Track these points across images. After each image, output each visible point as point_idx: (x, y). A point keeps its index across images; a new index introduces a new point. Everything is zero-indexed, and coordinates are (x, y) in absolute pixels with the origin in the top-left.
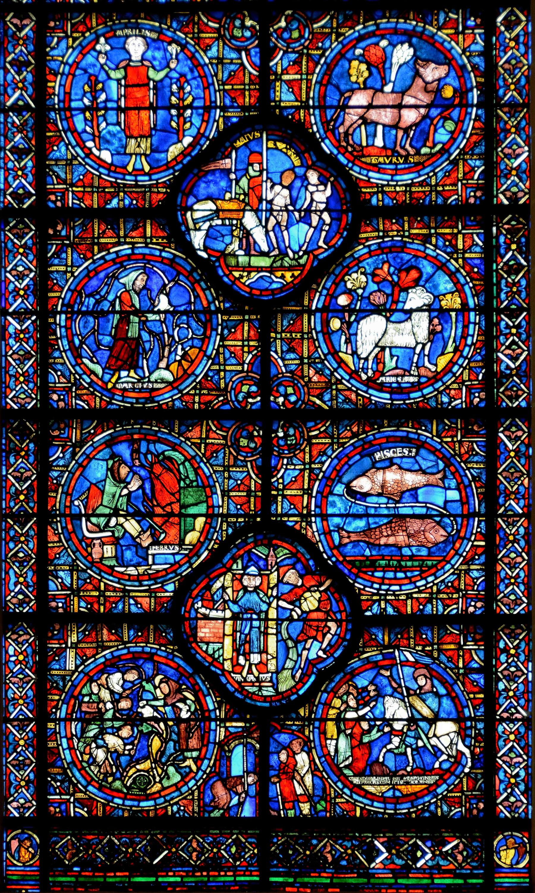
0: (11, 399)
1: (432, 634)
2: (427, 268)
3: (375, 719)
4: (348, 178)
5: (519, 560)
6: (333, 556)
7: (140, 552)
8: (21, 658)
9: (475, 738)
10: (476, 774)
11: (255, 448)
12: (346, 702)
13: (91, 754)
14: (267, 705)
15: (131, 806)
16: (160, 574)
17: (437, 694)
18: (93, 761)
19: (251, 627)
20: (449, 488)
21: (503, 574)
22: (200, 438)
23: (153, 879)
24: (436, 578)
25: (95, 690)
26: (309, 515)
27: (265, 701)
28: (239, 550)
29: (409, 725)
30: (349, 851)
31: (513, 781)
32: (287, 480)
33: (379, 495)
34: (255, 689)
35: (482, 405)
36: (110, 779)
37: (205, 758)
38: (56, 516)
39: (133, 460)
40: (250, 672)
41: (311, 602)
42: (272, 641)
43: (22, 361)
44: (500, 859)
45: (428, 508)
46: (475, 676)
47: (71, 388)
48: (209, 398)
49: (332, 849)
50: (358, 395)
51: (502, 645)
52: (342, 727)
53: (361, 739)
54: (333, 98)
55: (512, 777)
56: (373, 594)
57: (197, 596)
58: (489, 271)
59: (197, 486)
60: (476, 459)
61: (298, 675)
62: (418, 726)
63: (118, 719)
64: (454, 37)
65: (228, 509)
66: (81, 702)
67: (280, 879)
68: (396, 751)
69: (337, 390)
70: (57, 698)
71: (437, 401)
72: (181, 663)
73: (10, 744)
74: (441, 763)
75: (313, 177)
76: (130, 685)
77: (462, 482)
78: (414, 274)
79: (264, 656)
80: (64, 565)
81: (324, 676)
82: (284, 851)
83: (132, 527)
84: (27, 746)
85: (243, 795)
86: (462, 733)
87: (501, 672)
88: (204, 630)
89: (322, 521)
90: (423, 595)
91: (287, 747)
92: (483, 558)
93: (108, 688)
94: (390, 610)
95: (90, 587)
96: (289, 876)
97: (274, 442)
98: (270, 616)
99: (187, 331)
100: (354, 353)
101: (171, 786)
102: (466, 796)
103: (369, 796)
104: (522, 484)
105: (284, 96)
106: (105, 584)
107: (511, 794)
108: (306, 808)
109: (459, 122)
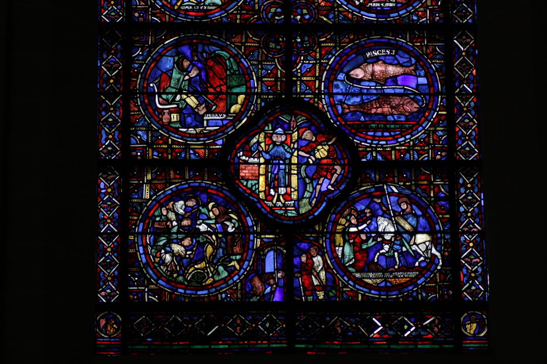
0: (104, 16)
1: (411, 174)
3: (371, 232)
5: (471, 124)
6: (338, 121)
7: (197, 118)
8: (109, 190)
9: (444, 245)
10: (446, 270)
11: (281, 49)
12: (349, 221)
13: (161, 258)
14: (292, 222)
15: (191, 294)
16: (212, 133)
18: (163, 262)
19: (279, 169)
20: (420, 76)
21: (460, 133)
22: (241, 42)
23: (207, 347)
24: (412, 136)
25: (164, 213)
26: (320, 93)
27: (289, 220)
28: (269, 117)
29: (395, 237)
30: (354, 326)
31: (473, 275)
32: (304, 71)
33: (370, 80)
34: (282, 212)
35: (441, 22)
36: (175, 275)
37: (246, 260)
38: (137, 94)
39: (192, 56)
40: (278, 200)
41: (322, 152)
42: (294, 180)
44: (466, 330)
45: (405, 89)
46: (443, 203)
47: (148, 8)
48: (247, 16)
49: (341, 324)
50: (353, 14)
51: (461, 181)
52: (347, 238)
53: (361, 246)
55: (472, 272)
56: (367, 147)
57: (239, 148)
59: (239, 74)
60: (438, 57)
61: (314, 202)
62: (402, 237)
63: (181, 233)
65: (262, 89)
66: (154, 221)
67: (303, 346)
68: (387, 255)
69: (338, 11)
70: (136, 218)
71: (409, 19)
72: (228, 194)
73: (100, 251)
74: (420, 263)
76: (190, 209)
77: (429, 72)
79: (289, 189)
80: (142, 126)
83: (192, 101)
84: (113, 251)
85: (275, 286)
86: (434, 242)
87: (461, 200)
88: (244, 171)
89: (329, 98)
90: (403, 148)
91: (307, 252)
92: (445, 122)
93: (174, 211)
94: (379, 157)
95: (161, 142)
96: (310, 344)
97: (294, 45)
98: (293, 162)
102: (439, 286)
103: (368, 286)
104: (472, 73)
106: (172, 140)
107: (473, 284)
108: (321, 295)
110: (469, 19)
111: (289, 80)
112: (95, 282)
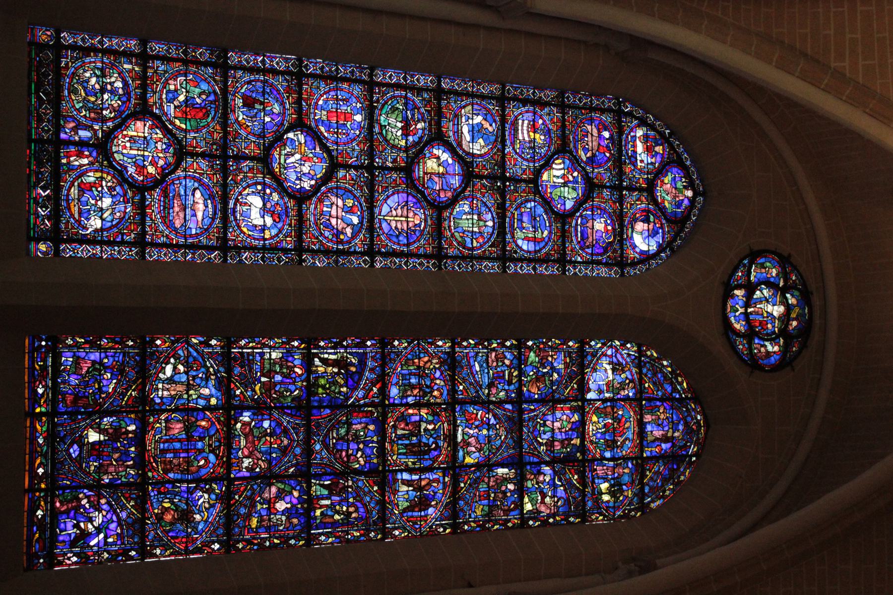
2: (280, 225)
4: (313, 196)
17: (112, 221)
18: (85, 71)
25: (116, 75)
41: (151, 170)
42: (135, 152)
43: (246, 60)
54: (341, 192)
58: (279, 250)
64: (361, 240)
75: (313, 182)
78: (277, 220)
81: (120, 173)
82: (45, 150)
83: (182, 98)
86: (96, 230)
91: (90, 155)
99: (257, 129)
100: (248, 194)
101: (74, 103)
105: (341, 173)
108: (64, 161)
109: (331, 241)
110: (229, 261)
111: (193, 155)
112: (73, 30)
